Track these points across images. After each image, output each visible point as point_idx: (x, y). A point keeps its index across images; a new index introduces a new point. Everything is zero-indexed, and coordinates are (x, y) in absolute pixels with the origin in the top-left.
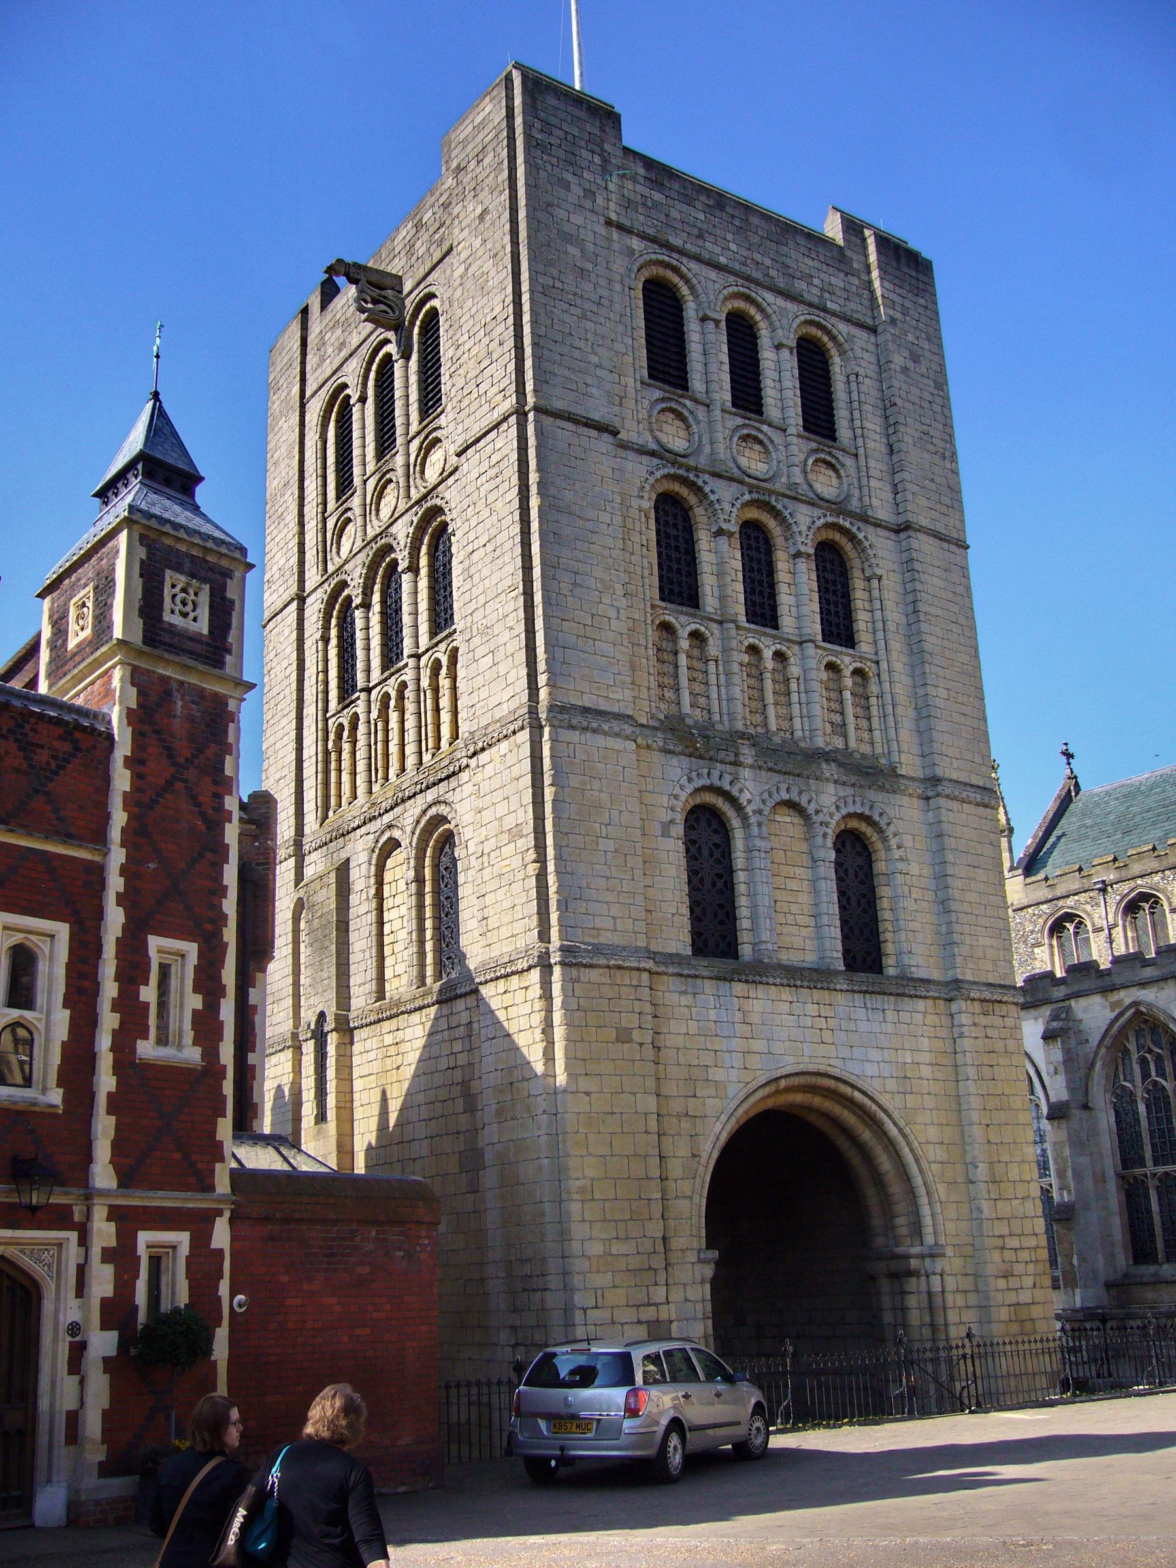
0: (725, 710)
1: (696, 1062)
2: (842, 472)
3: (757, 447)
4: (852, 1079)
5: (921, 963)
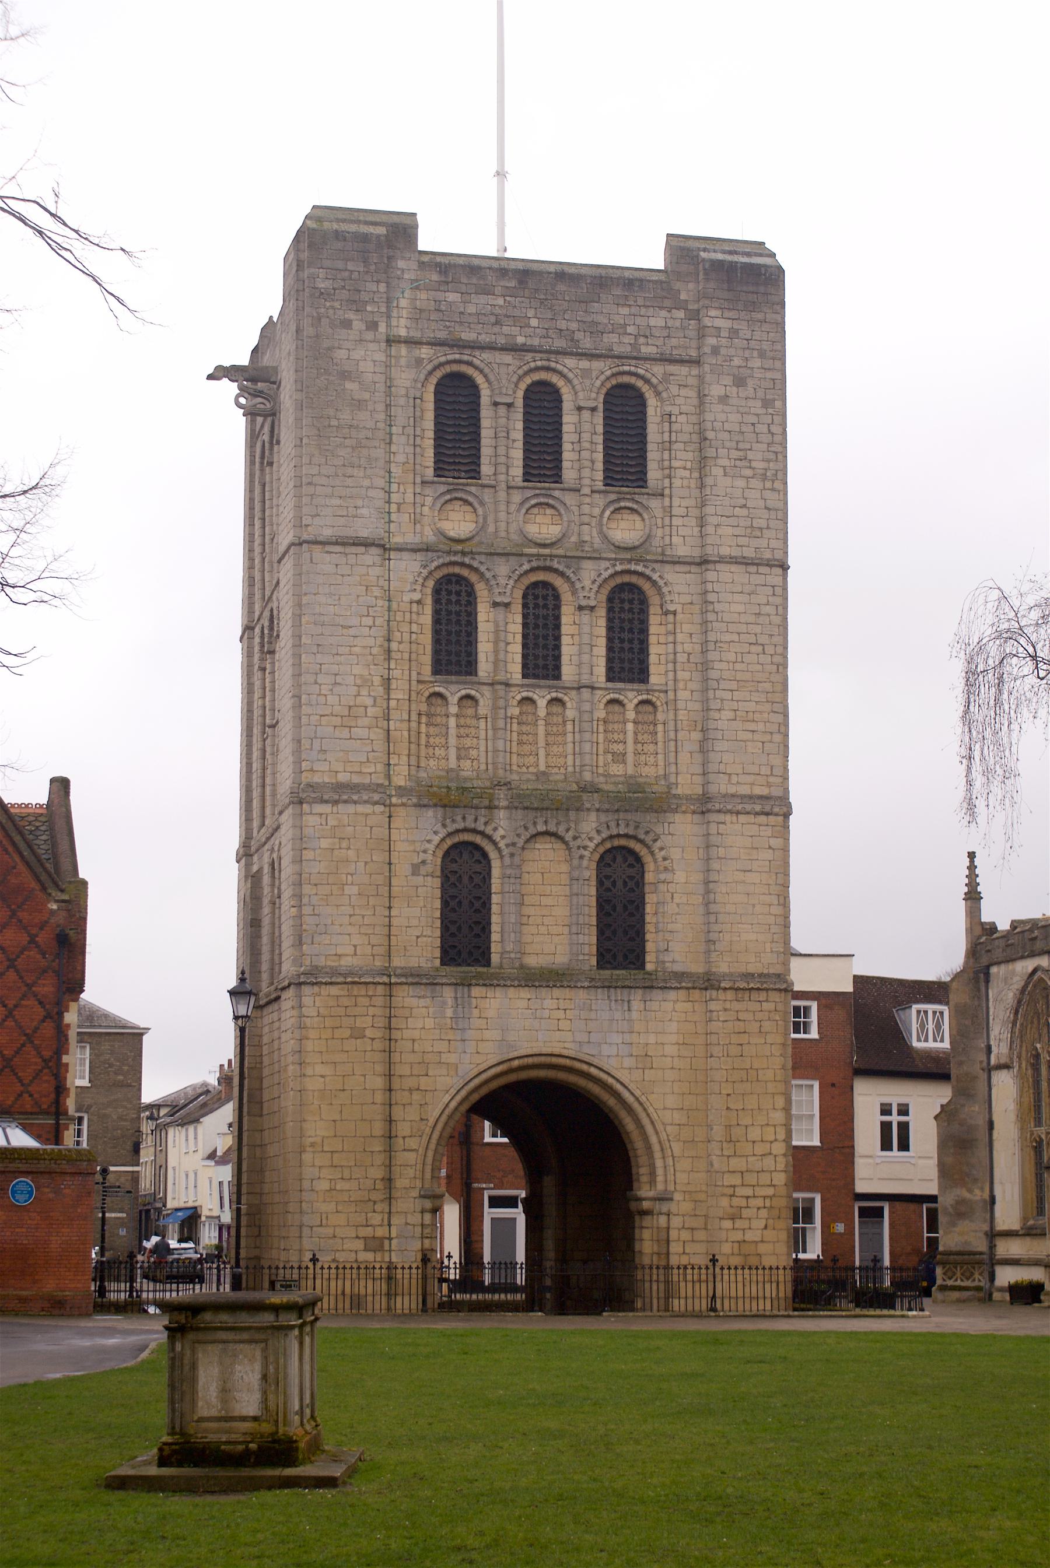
0: (490, 761)
1: (431, 1049)
2: (646, 516)
3: (549, 511)
4: (587, 1058)
5: (678, 958)
